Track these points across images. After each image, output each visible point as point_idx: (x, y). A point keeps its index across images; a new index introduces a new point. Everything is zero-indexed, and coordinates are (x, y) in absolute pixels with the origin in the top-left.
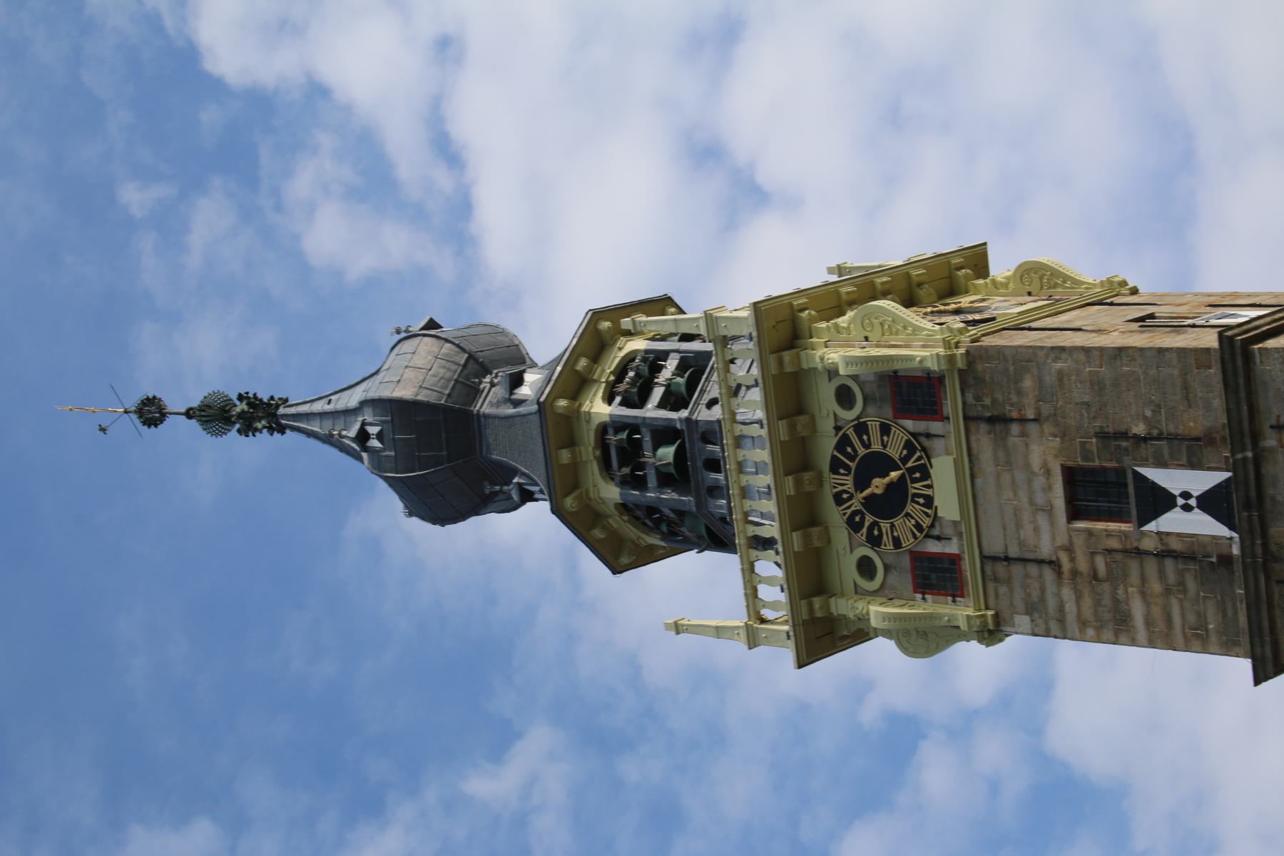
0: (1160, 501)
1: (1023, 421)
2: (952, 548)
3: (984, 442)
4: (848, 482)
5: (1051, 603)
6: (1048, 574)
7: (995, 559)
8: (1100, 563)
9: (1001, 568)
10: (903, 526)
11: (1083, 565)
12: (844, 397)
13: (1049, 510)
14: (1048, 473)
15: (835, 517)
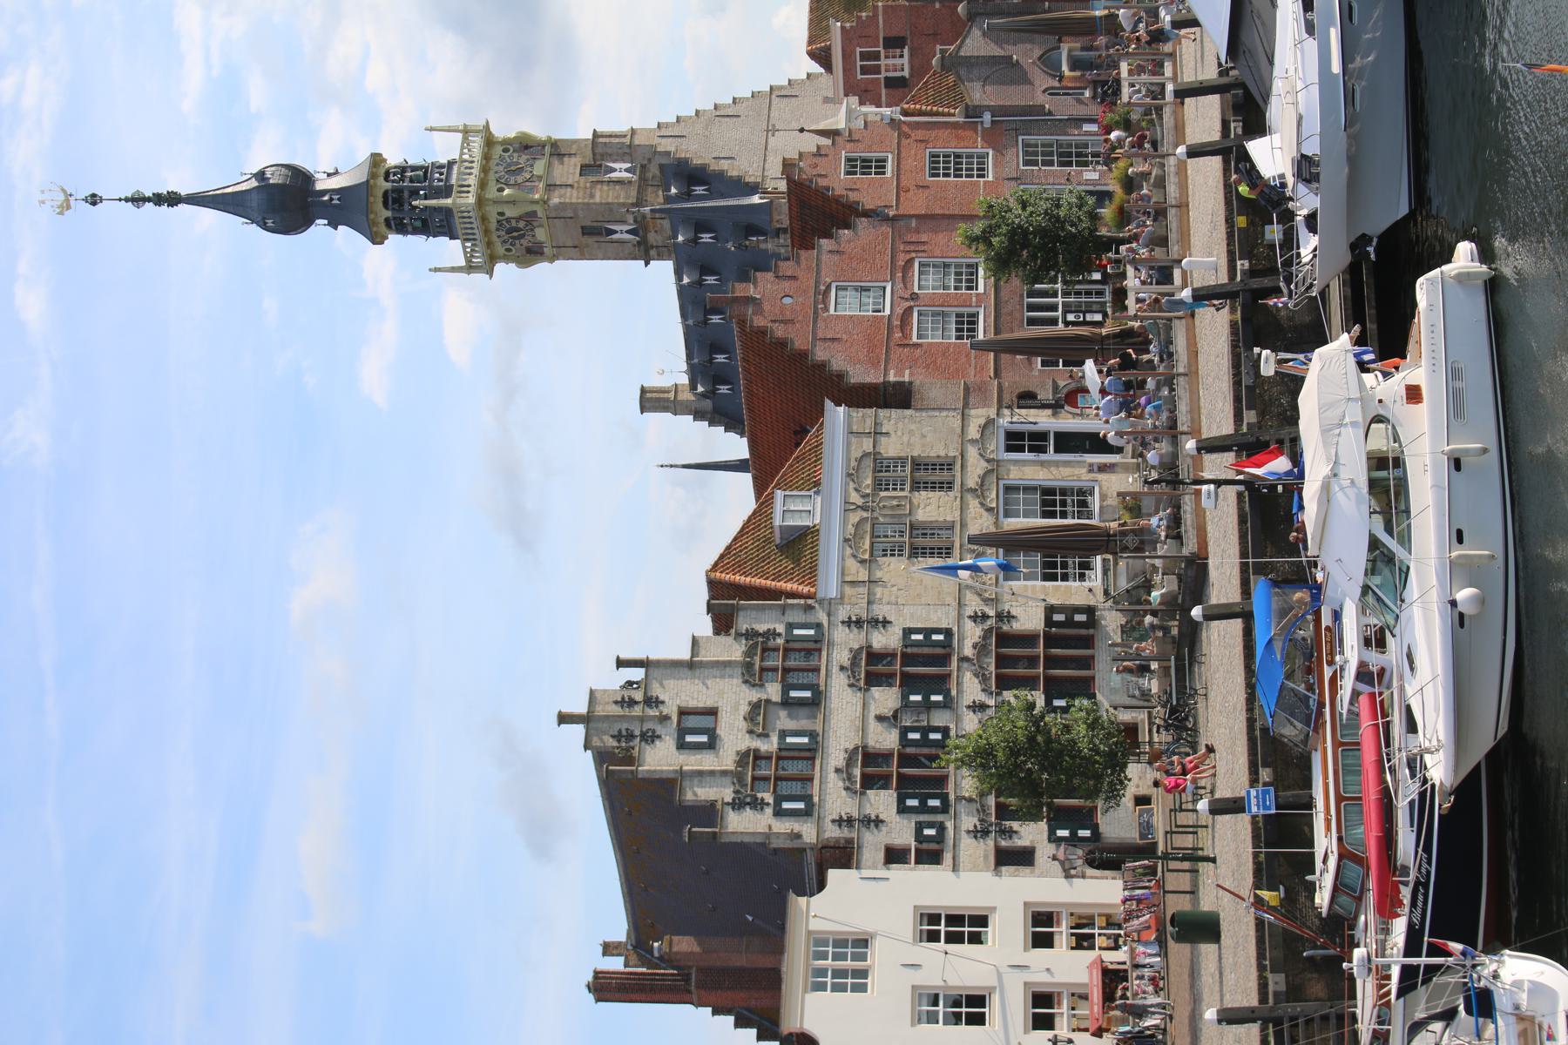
0: (614, 170)
1: (570, 155)
2: (536, 184)
3: (556, 162)
4: (501, 168)
5: (568, 194)
6: (569, 189)
7: (550, 185)
8: (588, 185)
9: (552, 188)
10: (520, 179)
11: (582, 185)
12: (506, 150)
13: (574, 174)
14: (575, 165)
15: (492, 177)
